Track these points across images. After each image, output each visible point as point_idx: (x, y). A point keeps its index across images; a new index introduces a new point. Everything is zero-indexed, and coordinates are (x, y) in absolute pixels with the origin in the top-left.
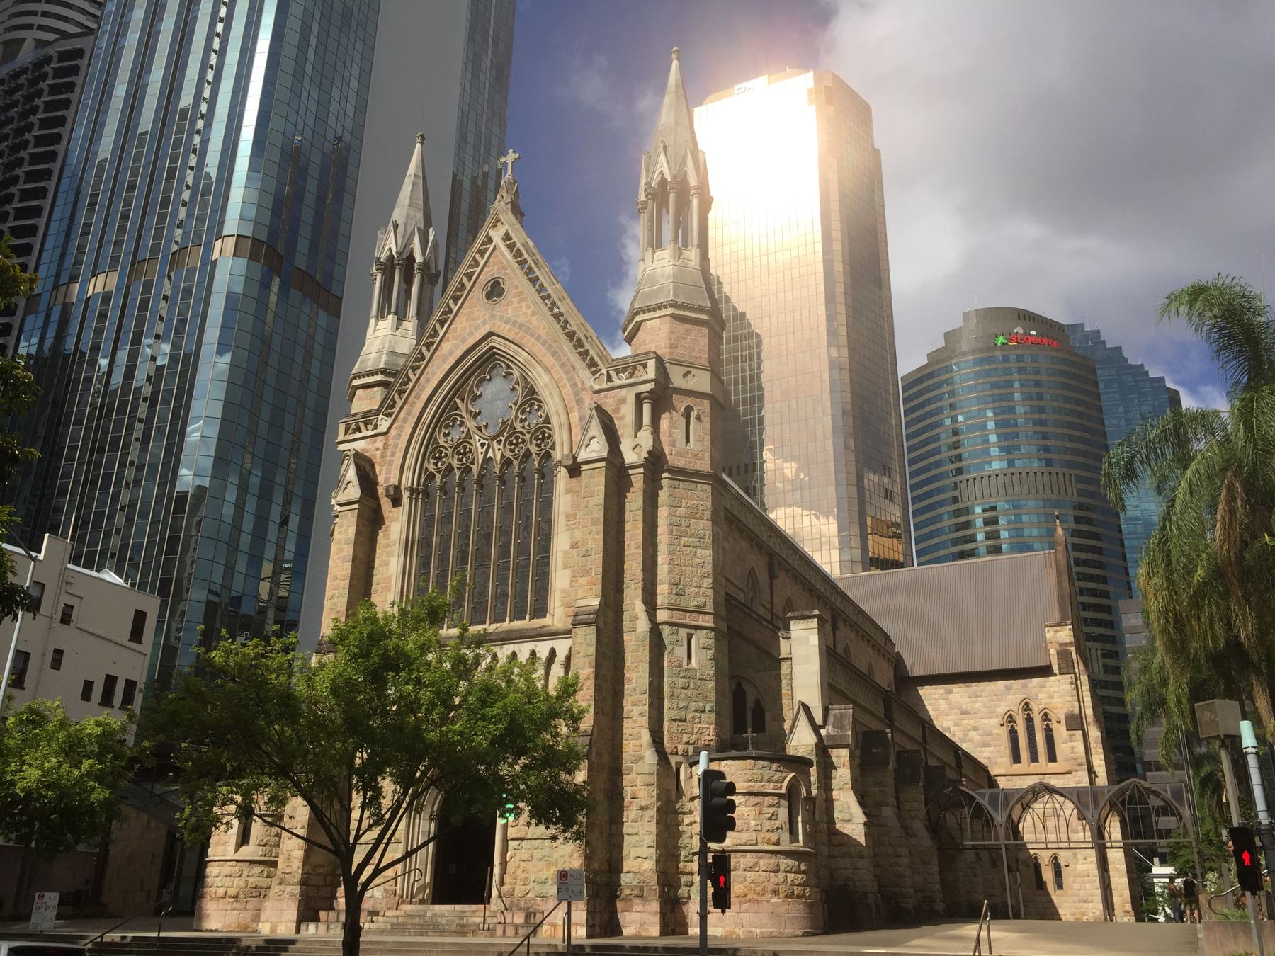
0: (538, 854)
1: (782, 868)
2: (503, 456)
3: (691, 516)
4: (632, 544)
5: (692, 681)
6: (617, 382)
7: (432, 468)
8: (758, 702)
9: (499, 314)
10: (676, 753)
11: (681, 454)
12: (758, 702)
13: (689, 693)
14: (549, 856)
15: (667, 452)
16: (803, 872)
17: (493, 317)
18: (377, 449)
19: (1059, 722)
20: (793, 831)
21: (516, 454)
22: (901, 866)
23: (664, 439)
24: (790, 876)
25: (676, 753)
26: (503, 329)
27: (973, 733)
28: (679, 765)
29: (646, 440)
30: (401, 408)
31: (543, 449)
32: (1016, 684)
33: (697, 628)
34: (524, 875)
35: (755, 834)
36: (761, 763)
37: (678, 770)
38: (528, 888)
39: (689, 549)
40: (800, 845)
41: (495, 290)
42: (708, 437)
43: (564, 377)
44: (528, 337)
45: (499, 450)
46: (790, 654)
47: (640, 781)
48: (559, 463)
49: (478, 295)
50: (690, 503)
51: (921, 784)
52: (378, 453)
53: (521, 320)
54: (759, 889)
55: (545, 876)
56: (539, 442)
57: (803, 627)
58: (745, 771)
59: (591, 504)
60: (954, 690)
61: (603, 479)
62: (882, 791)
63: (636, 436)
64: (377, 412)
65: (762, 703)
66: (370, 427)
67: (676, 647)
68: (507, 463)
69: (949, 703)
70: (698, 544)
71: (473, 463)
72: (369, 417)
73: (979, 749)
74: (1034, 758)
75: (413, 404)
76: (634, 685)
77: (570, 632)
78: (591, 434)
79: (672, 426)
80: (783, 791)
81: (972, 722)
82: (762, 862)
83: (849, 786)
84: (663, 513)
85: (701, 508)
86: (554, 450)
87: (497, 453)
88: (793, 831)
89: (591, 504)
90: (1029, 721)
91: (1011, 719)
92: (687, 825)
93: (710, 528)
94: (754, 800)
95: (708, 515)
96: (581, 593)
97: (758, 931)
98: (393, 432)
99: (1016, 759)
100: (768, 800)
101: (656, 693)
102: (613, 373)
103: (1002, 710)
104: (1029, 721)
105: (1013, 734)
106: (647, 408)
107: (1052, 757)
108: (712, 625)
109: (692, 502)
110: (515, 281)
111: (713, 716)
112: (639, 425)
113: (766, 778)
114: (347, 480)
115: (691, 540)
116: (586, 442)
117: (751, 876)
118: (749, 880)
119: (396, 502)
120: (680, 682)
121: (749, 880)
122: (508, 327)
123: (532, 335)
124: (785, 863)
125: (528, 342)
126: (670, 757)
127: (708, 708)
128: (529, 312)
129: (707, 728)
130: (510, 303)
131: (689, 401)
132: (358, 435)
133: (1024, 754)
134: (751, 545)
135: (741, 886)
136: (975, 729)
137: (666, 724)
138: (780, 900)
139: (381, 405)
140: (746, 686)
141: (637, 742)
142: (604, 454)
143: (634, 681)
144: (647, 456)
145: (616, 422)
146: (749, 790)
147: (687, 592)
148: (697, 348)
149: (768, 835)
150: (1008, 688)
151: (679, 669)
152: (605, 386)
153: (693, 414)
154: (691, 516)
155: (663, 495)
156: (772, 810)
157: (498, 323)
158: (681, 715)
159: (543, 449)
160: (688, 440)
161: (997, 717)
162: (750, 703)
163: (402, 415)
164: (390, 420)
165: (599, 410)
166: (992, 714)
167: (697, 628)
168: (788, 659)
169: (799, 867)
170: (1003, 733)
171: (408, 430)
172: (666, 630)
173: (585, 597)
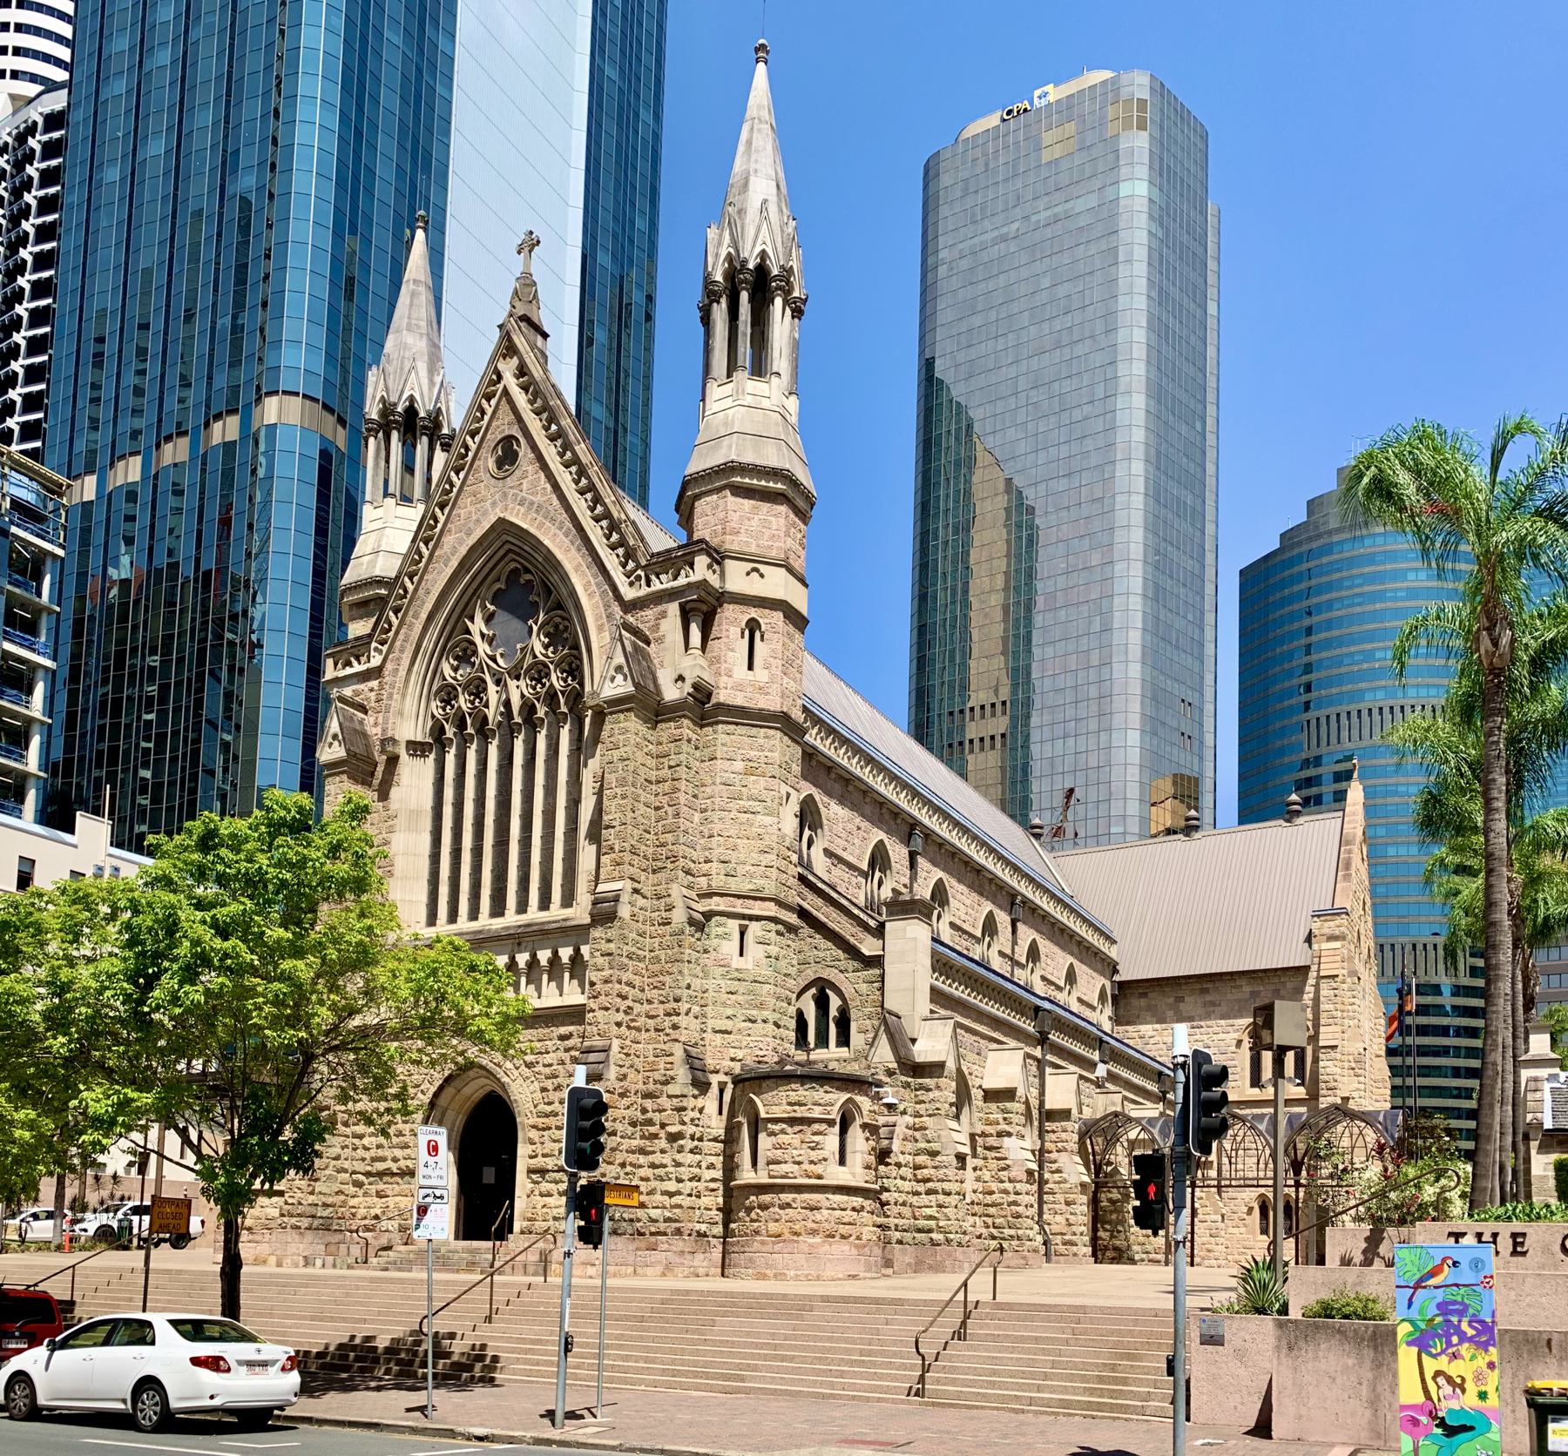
3: (749, 772)
7: (438, 713)
11: (739, 687)
13: (740, 998)
18: (372, 690)
30: (397, 633)
33: (752, 918)
52: (373, 695)
64: (370, 636)
66: (363, 659)
71: (487, 706)
72: (364, 642)
75: (411, 625)
85: (763, 760)
87: (517, 691)
98: (389, 666)
109: (753, 753)
114: (332, 731)
119: (393, 761)
131: (754, 613)
132: (348, 671)
139: (374, 629)
141: (669, 1059)
148: (767, 533)
160: (750, 667)
163: (398, 643)
164: (385, 648)
167: (752, 918)
171: (406, 662)
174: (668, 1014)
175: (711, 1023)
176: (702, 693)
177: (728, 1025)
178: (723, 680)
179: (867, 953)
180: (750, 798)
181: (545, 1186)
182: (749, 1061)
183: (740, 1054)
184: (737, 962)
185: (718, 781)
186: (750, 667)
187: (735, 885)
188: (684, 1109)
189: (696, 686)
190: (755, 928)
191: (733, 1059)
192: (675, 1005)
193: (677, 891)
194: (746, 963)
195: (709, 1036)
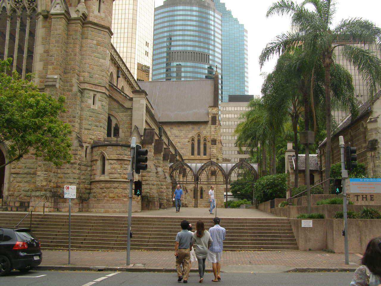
0: (25, 180)
2: (11, 7)
3: (98, 44)
8: (116, 125)
11: (96, 17)
14: (30, 181)
19: (209, 141)
21: (18, 7)
22: (162, 189)
31: (31, 6)
32: (196, 127)
34: (18, 188)
38: (20, 193)
45: (9, 3)
46: (132, 107)
48: (40, 14)
51: (169, 160)
55: (28, 188)
56: (29, 3)
57: (138, 96)
58: (116, 151)
59: (55, 34)
62: (158, 162)
65: (118, 126)
68: (14, 11)
74: (199, 154)
77: (44, 89)
86: (37, 7)
89: (55, 34)
90: (199, 141)
91: (193, 140)
92: (89, 171)
94: (119, 162)
96: (49, 73)
97: (118, 210)
99: (193, 154)
103: (190, 136)
104: (199, 141)
105: (193, 145)
107: (205, 154)
133: (196, 152)
134: (112, 63)
135: (112, 194)
138: (127, 200)
140: (112, 118)
143: (70, 112)
144: (82, 15)
150: (193, 128)
151: (90, 108)
154: (98, 44)
156: (126, 166)
159: (31, 6)
161: (188, 139)
162: (113, 125)
166: (186, 137)
167: (97, 92)
168: (130, 108)
170: (190, 145)
173: (51, 74)
174: (70, 122)
175: (84, 126)
176: (85, 16)
177: (89, 127)
178: (91, 14)
179: (126, 107)
180: (98, 53)
181: (19, 179)
182: (96, 139)
183: (93, 137)
184: (92, 107)
185: (88, 46)
186: (99, 12)
187: (92, 81)
188: (77, 154)
189: (83, 14)
190: (98, 96)
191: (90, 139)
192: (72, 119)
193: (74, 81)
194: (96, 107)
195: (83, 130)
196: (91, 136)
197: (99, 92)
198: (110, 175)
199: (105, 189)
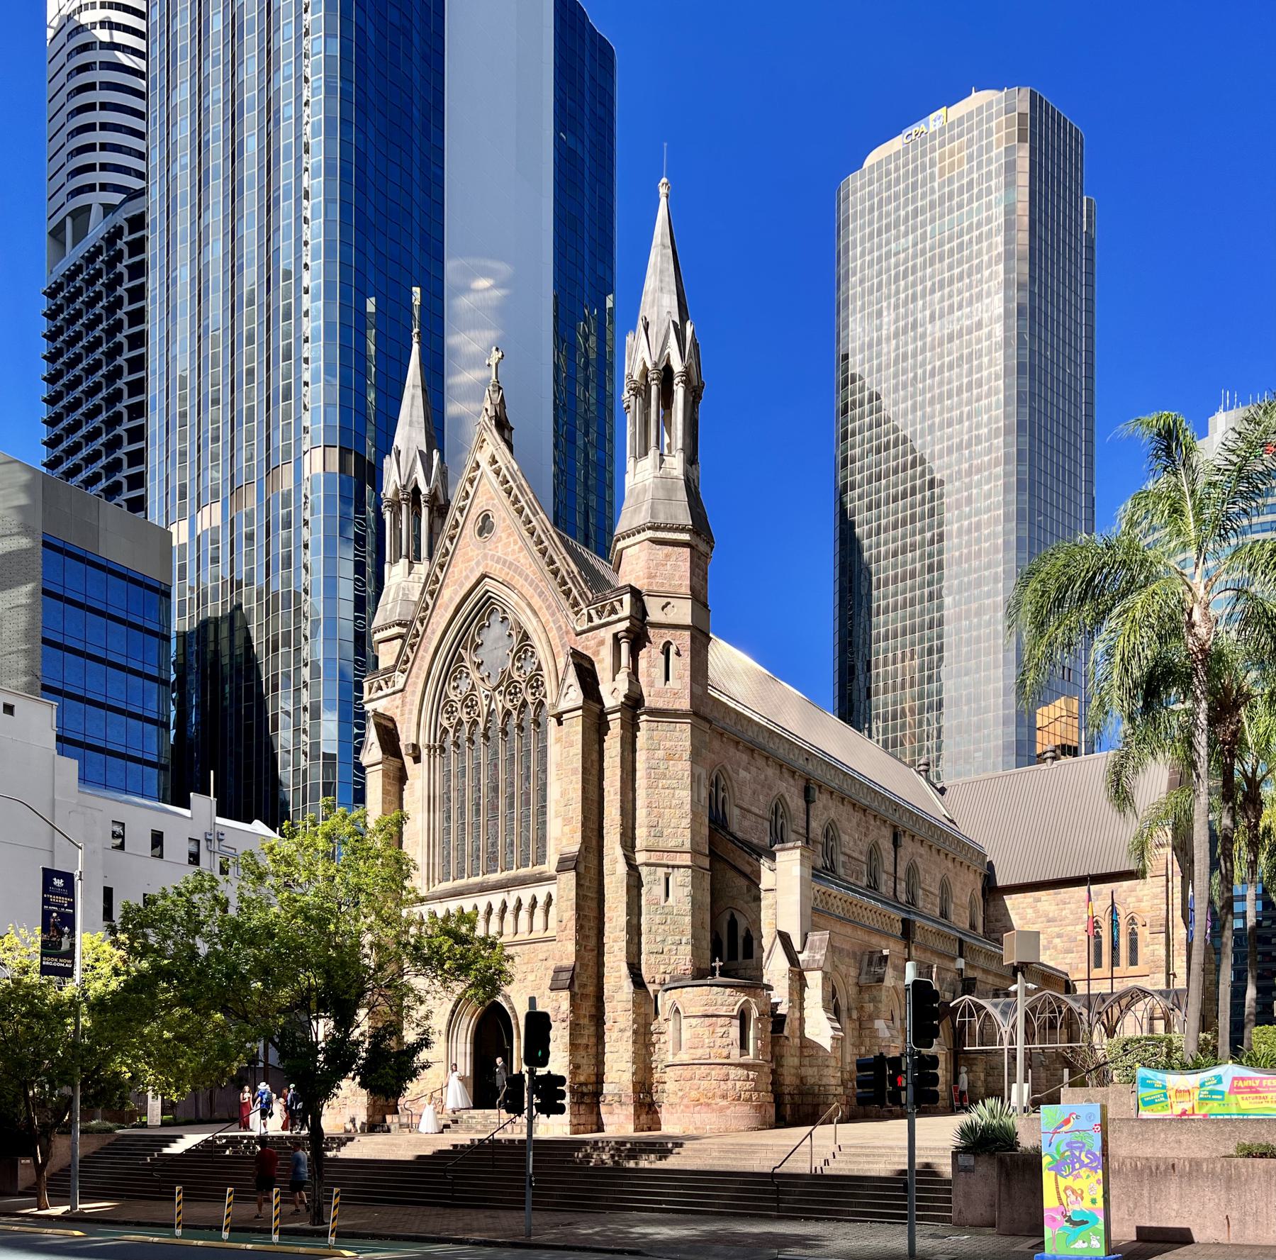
1: (731, 1077)
3: (669, 757)
4: (612, 789)
5: (669, 917)
6: (597, 621)
8: (748, 931)
9: (491, 553)
10: (654, 982)
11: (659, 695)
12: (748, 931)
13: (667, 928)
15: (645, 694)
16: (752, 1080)
17: (485, 556)
20: (744, 1045)
23: (643, 679)
24: (739, 1084)
25: (654, 982)
26: (495, 569)
27: (1057, 941)
28: (656, 992)
29: (622, 684)
35: (708, 1050)
36: (728, 990)
37: (656, 997)
39: (667, 791)
40: (750, 1057)
41: (485, 526)
42: (688, 673)
43: (551, 619)
44: (517, 577)
47: (620, 1006)
49: (470, 530)
50: (668, 744)
53: (510, 558)
54: (710, 1095)
60: (1043, 898)
61: (580, 728)
63: (614, 680)
67: (654, 887)
69: (1036, 911)
70: (675, 786)
73: (1061, 956)
76: (614, 924)
78: (568, 682)
79: (650, 666)
80: (735, 1013)
81: (1057, 929)
82: (713, 1073)
83: (820, 1004)
84: (641, 757)
88: (744, 1045)
93: (689, 768)
95: (687, 755)
100: (721, 1021)
101: (634, 931)
102: (593, 612)
106: (625, 647)
108: (689, 863)
110: (503, 516)
111: (689, 947)
112: (617, 668)
113: (719, 1002)
115: (669, 782)
116: (565, 691)
117: (704, 1084)
118: (702, 1088)
120: (657, 919)
121: (702, 1088)
122: (499, 566)
123: (521, 575)
124: (734, 1073)
125: (519, 582)
126: (648, 985)
127: (684, 941)
128: (516, 548)
129: (683, 959)
130: (500, 539)
136: (1059, 936)
137: (643, 957)
140: (737, 916)
142: (580, 702)
144: (623, 700)
145: (597, 666)
146: (704, 1013)
147: (665, 833)
149: (720, 1051)
152: (585, 627)
153: (673, 649)
155: (642, 737)
156: (723, 1030)
157: (490, 563)
158: (655, 948)
160: (667, 678)
162: (741, 933)
165: (576, 654)
167: (673, 867)
169: (748, 1075)
172: (644, 871)
180: (670, 778)
186: (667, 678)
187: (662, 844)
196: (662, 967)
197: (679, 867)
198: (692, 1051)
199: (683, 1082)
